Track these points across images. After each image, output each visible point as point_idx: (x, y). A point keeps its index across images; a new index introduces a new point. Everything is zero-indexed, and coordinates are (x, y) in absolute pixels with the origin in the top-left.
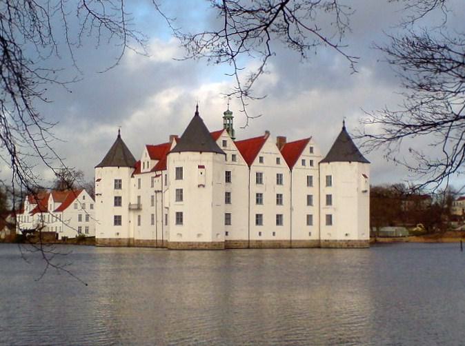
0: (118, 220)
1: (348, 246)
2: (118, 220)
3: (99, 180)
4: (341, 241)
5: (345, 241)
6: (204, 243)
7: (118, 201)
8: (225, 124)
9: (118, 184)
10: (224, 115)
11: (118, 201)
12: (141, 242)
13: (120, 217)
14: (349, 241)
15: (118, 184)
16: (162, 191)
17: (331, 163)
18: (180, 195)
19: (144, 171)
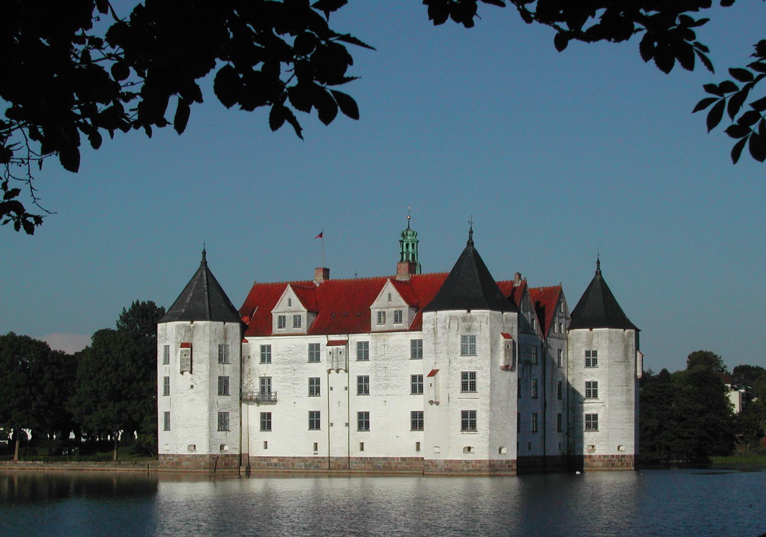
6: (508, 461)
16: (347, 371)
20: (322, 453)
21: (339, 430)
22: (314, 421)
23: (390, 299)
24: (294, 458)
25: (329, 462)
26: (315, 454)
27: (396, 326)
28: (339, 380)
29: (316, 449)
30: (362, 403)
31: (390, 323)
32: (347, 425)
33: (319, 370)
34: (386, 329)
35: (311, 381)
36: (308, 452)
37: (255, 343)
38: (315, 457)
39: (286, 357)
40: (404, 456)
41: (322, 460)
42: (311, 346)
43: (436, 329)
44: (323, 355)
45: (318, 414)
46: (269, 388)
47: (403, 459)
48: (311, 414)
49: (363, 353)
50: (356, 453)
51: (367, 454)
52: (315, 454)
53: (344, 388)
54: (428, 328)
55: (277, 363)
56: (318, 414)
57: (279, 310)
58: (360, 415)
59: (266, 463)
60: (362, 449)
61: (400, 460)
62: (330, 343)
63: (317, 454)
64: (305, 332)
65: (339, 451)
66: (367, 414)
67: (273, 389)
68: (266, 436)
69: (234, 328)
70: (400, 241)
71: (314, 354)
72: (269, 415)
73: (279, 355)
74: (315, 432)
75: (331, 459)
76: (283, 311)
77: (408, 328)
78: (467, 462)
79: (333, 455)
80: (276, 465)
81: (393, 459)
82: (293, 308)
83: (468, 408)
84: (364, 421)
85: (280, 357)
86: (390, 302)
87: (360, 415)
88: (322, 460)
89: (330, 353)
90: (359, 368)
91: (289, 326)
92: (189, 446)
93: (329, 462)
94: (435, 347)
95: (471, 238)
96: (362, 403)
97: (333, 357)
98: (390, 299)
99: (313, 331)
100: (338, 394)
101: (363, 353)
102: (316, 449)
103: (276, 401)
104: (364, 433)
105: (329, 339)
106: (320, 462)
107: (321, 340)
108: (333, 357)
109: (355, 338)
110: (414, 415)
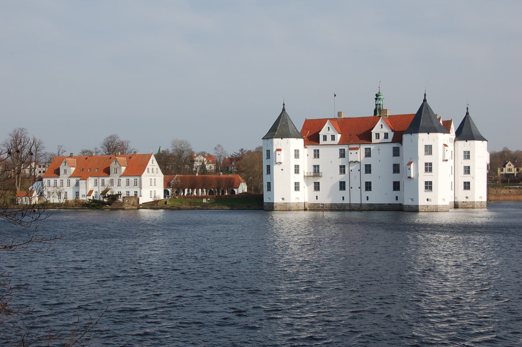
0: (297, 187)
1: (481, 206)
2: (297, 187)
3: (280, 150)
4: (477, 202)
5: (479, 202)
6: (446, 206)
7: (297, 169)
8: (376, 105)
9: (297, 155)
10: (375, 97)
11: (297, 169)
12: (321, 205)
13: (298, 183)
14: (481, 202)
15: (297, 155)
17: (469, 142)
18: (429, 168)
20: (346, 201)
25: (350, 206)
26: (343, 202)
29: (343, 199)
30: (367, 178)
37: (311, 149)
38: (343, 204)
41: (347, 205)
45: (344, 182)
46: (318, 170)
47: (388, 204)
50: (365, 201)
52: (343, 202)
56: (344, 182)
58: (366, 183)
59: (317, 206)
62: (351, 149)
65: (356, 200)
66: (370, 183)
67: (320, 171)
68: (317, 193)
69: (301, 141)
70: (375, 99)
71: (342, 154)
72: (319, 183)
78: (427, 206)
79: (352, 202)
81: (384, 204)
83: (428, 180)
84: (368, 186)
87: (366, 183)
88: (347, 205)
91: (329, 141)
96: (367, 178)
100: (355, 174)
103: (322, 176)
105: (350, 147)
106: (346, 206)
107: (346, 147)
109: (363, 148)
110: (395, 183)
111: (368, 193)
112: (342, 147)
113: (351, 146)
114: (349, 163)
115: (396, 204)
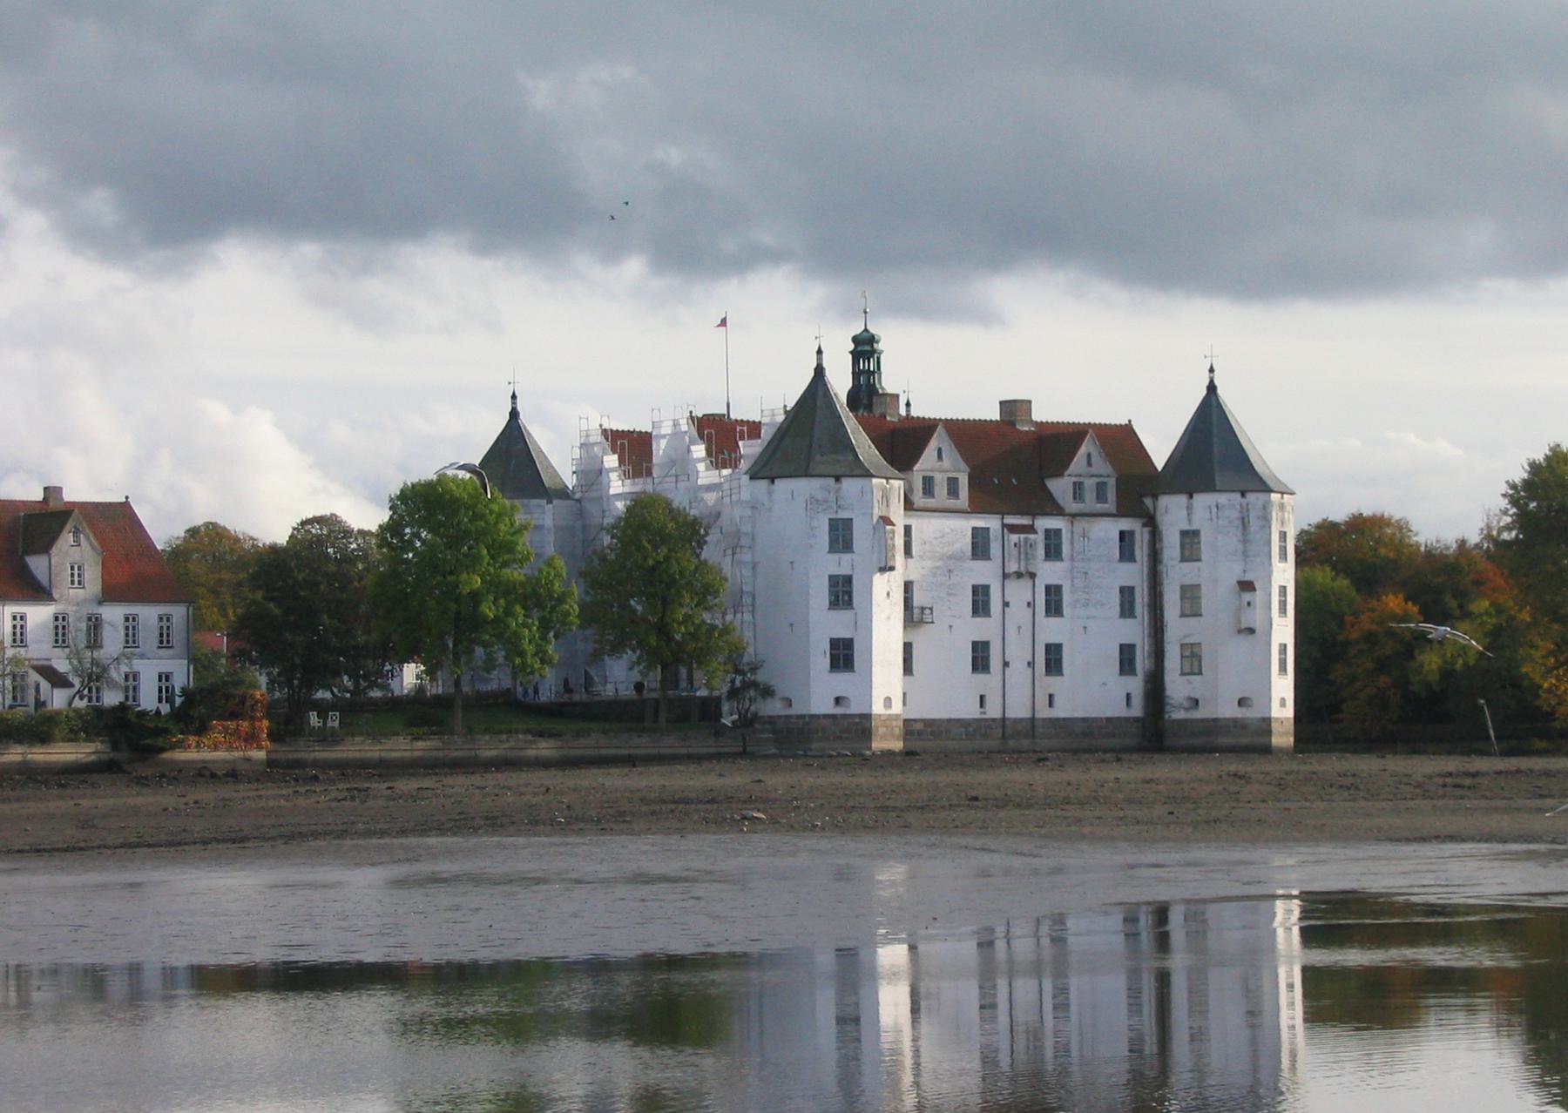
16: (1033, 576)
19: (930, 502)
20: (993, 711)
21: (1019, 676)
22: (980, 658)
23: (1089, 464)
24: (949, 721)
25: (1004, 727)
27: (1100, 507)
28: (1019, 592)
30: (1052, 629)
31: (1090, 503)
32: (1006, 664)
33: (985, 573)
34: (1087, 510)
35: (975, 589)
36: (970, 711)
39: (938, 549)
40: (1109, 714)
42: (976, 532)
43: (1246, 520)
44: (995, 548)
47: (1109, 719)
48: (975, 645)
49: (1053, 550)
50: (1044, 712)
51: (1062, 711)
52: (982, 713)
53: (1026, 603)
54: (1228, 517)
55: (921, 557)
57: (923, 467)
58: (1048, 647)
60: (1051, 704)
61: (1104, 721)
63: (984, 713)
64: (1114, 511)
66: (1058, 647)
71: (980, 546)
73: (925, 543)
74: (981, 677)
75: (1007, 723)
76: (929, 468)
77: (1114, 511)
79: (1011, 714)
80: (920, 733)
82: (1094, 470)
84: (1054, 659)
85: (927, 547)
86: (1090, 469)
87: (1048, 647)
89: (1015, 545)
90: (1050, 573)
92: (791, 701)
93: (1004, 727)
94: (1245, 547)
95: (1212, 381)
96: (1052, 629)
97: (1020, 553)
98: (1089, 464)
99: (976, 507)
100: (1019, 613)
101: (1053, 550)
102: (982, 705)
104: (1052, 680)
107: (992, 523)
108: (1020, 553)
111: (1049, 684)
112: (980, 522)
113: (1010, 520)
114: (1005, 576)
115: (1127, 719)
